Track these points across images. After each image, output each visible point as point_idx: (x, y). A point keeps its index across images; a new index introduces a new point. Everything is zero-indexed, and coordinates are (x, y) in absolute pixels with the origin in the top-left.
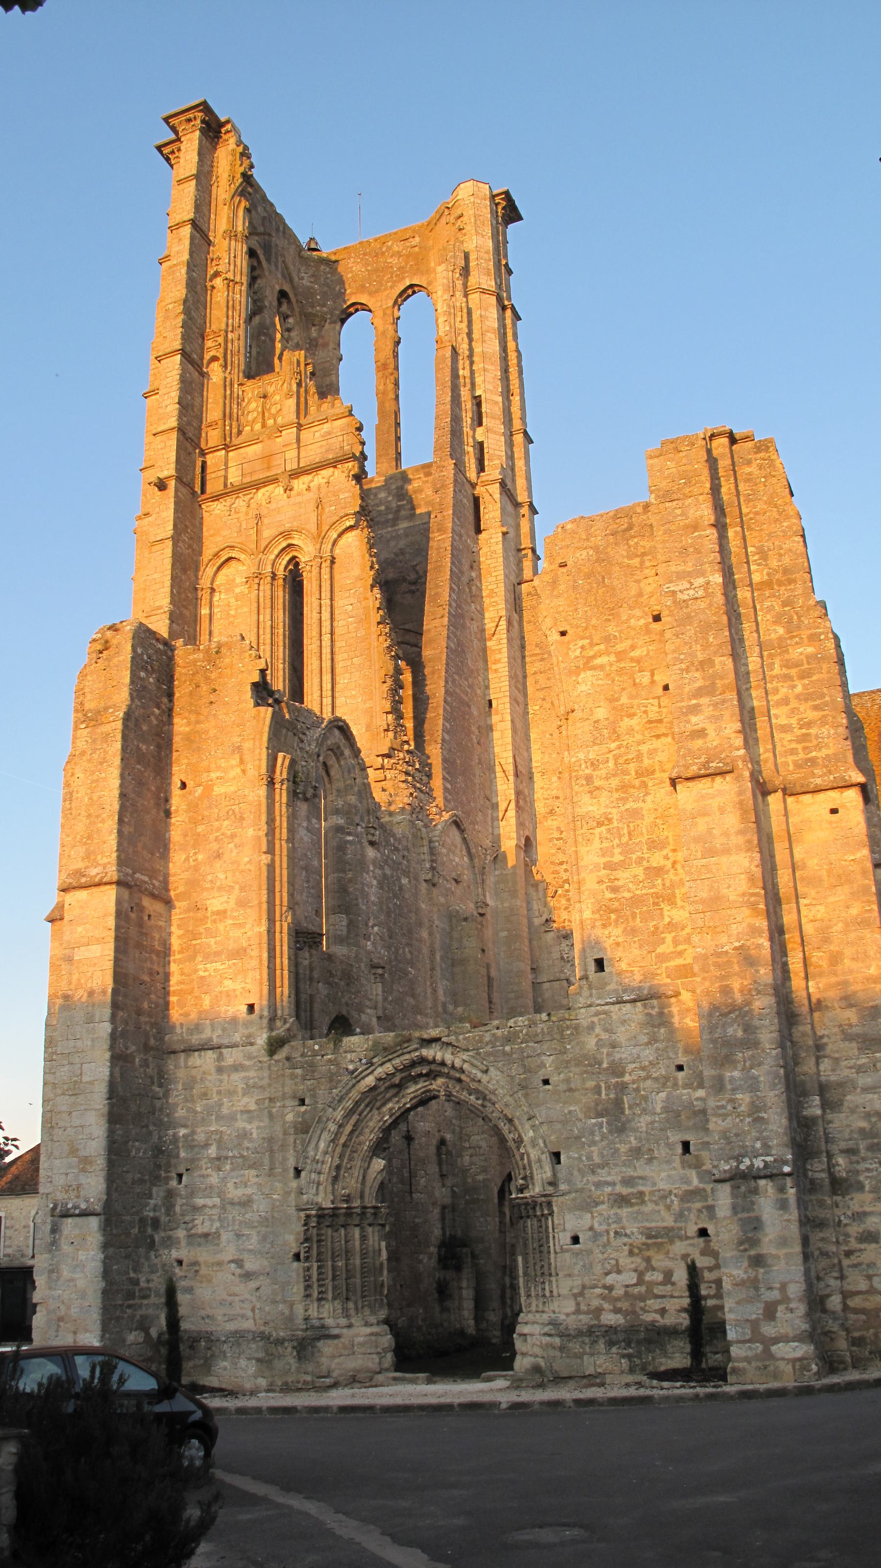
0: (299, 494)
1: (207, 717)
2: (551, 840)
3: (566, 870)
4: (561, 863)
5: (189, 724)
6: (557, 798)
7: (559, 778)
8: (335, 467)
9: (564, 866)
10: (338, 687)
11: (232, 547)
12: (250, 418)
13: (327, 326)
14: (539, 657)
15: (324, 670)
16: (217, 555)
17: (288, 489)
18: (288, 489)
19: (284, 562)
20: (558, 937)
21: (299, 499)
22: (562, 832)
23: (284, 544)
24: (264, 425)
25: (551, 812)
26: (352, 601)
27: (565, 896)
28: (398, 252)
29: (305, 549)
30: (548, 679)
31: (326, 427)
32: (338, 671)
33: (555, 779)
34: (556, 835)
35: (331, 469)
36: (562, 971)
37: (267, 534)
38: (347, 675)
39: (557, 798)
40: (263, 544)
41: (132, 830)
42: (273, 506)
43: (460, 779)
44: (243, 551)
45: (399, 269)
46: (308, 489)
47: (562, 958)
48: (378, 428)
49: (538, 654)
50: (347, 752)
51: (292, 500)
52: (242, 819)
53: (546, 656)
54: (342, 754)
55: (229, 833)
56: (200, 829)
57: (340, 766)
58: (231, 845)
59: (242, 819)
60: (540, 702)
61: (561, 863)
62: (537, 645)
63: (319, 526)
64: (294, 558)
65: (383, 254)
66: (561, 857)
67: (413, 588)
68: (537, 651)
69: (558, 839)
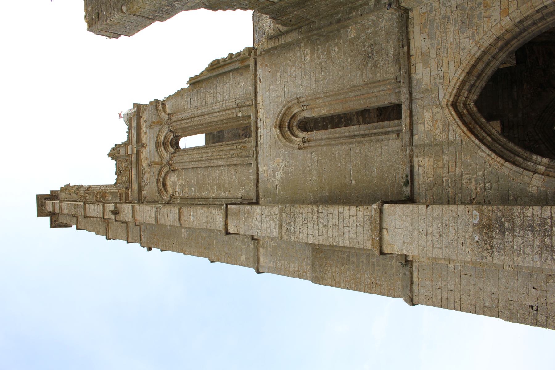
23: (162, 147)
51: (148, 144)
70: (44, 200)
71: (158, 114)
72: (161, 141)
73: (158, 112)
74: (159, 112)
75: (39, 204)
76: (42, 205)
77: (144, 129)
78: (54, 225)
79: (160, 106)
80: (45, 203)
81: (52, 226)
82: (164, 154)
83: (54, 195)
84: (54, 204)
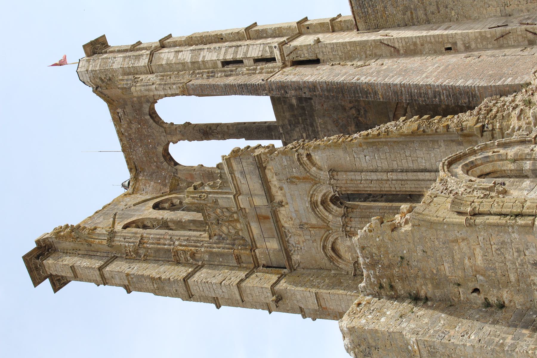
0: (285, 196)
1: (419, 269)
5: (426, 285)
8: (265, 168)
10: (428, 166)
11: (324, 247)
12: (233, 231)
13: (179, 175)
15: (414, 178)
16: (330, 259)
17: (281, 204)
18: (281, 204)
19: (335, 207)
21: (288, 195)
23: (321, 207)
24: (237, 221)
26: (362, 156)
28: (128, 124)
29: (324, 191)
30: (430, 4)
31: (237, 175)
32: (415, 166)
35: (267, 171)
37: (314, 221)
38: (419, 160)
40: (321, 223)
41: (510, 337)
42: (294, 215)
43: (505, 70)
44: (327, 238)
45: (139, 124)
46: (281, 189)
48: (247, 139)
49: (412, 13)
50: (472, 158)
51: (289, 201)
52: (503, 243)
53: (412, 6)
54: (472, 162)
55: (516, 254)
56: (513, 277)
57: (482, 164)
58: (527, 253)
59: (503, 243)
60: (448, 10)
62: (404, 14)
63: (305, 179)
64: (331, 200)
65: (130, 135)
67: (362, 112)
68: (409, 13)
70: (37, 261)
71: (305, 169)
72: (317, 201)
73: (303, 167)
74: (306, 167)
75: (31, 269)
76: (37, 268)
77: (274, 182)
78: (57, 288)
79: (305, 159)
80: (42, 265)
81: (56, 290)
82: (326, 216)
83: (43, 245)
84: (74, 268)
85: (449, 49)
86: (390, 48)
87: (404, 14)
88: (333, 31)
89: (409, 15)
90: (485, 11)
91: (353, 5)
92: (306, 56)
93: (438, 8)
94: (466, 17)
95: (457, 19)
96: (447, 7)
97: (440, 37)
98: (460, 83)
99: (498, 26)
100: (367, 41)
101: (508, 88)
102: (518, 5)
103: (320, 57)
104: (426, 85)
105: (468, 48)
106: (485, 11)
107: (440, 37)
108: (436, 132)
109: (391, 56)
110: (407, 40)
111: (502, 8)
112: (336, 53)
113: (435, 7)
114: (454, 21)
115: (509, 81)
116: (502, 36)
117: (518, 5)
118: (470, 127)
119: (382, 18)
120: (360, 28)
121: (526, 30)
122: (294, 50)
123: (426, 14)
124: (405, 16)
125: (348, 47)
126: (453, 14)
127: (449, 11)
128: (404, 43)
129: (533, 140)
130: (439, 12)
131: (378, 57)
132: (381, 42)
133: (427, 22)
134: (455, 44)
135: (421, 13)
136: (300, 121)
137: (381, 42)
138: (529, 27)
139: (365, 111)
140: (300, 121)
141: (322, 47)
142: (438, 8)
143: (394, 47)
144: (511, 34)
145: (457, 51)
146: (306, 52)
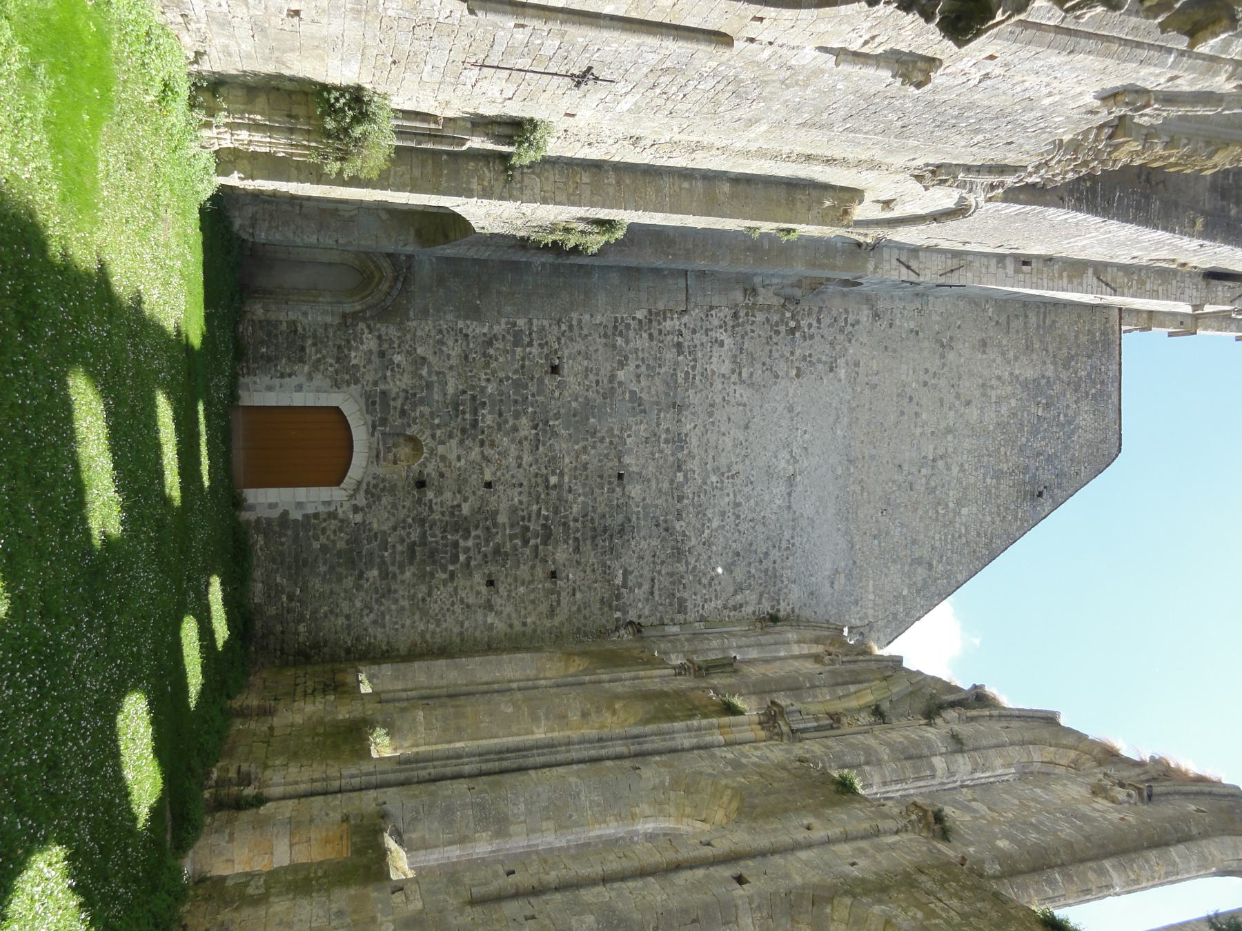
2: (846, 311)
3: (810, 326)
4: (819, 321)
6: (891, 325)
7: (911, 331)
9: (815, 324)
14: (1041, 323)
20: (736, 305)
22: (853, 325)
25: (877, 316)
27: (782, 320)
30: (1017, 331)
33: (912, 325)
34: (851, 319)
36: (696, 306)
39: (891, 325)
47: (712, 308)
49: (1044, 323)
60: (996, 318)
61: (819, 321)
62: (1054, 322)
66: (826, 321)
67: (1143, 177)
68: (1048, 322)
69: (846, 320)
85: (1025, 263)
86: (1104, 279)
87: (1054, 322)
88: (1151, 312)
89: (1047, 321)
90: (949, 307)
91: (1117, 348)
92: (1221, 288)
93: (1008, 323)
94: (975, 302)
95: (987, 302)
96: (997, 322)
97: (1034, 285)
98: (1081, 216)
99: (951, 286)
100: (1133, 296)
101: (1022, 197)
102: (904, 308)
103: (1202, 284)
104: (1127, 221)
105: (1001, 258)
106: (949, 307)
107: (1034, 285)
108: (1189, 140)
109: (1106, 265)
110: (1080, 288)
111: (925, 308)
112: (1179, 284)
113: (1012, 325)
114: (992, 299)
115: (1015, 208)
116: (952, 271)
117: (904, 308)
118: (1135, 140)
119: (1084, 322)
120: (1116, 312)
121: (918, 275)
122: (1235, 299)
123: (1026, 316)
124: (1053, 318)
125: (1160, 291)
126: (991, 310)
127: (995, 316)
128: (1085, 282)
129: (1152, 102)
130: (1008, 317)
131: (1126, 269)
132: (1115, 292)
133: (1027, 304)
134: (1017, 271)
135: (1033, 320)
136: (1231, 177)
137: (1115, 291)
138: (913, 278)
139: (1139, 177)
140: (1231, 177)
141: (1196, 298)
142: (1008, 323)
143: (1098, 278)
144: (940, 272)
145: (1016, 257)
146: (1219, 293)
